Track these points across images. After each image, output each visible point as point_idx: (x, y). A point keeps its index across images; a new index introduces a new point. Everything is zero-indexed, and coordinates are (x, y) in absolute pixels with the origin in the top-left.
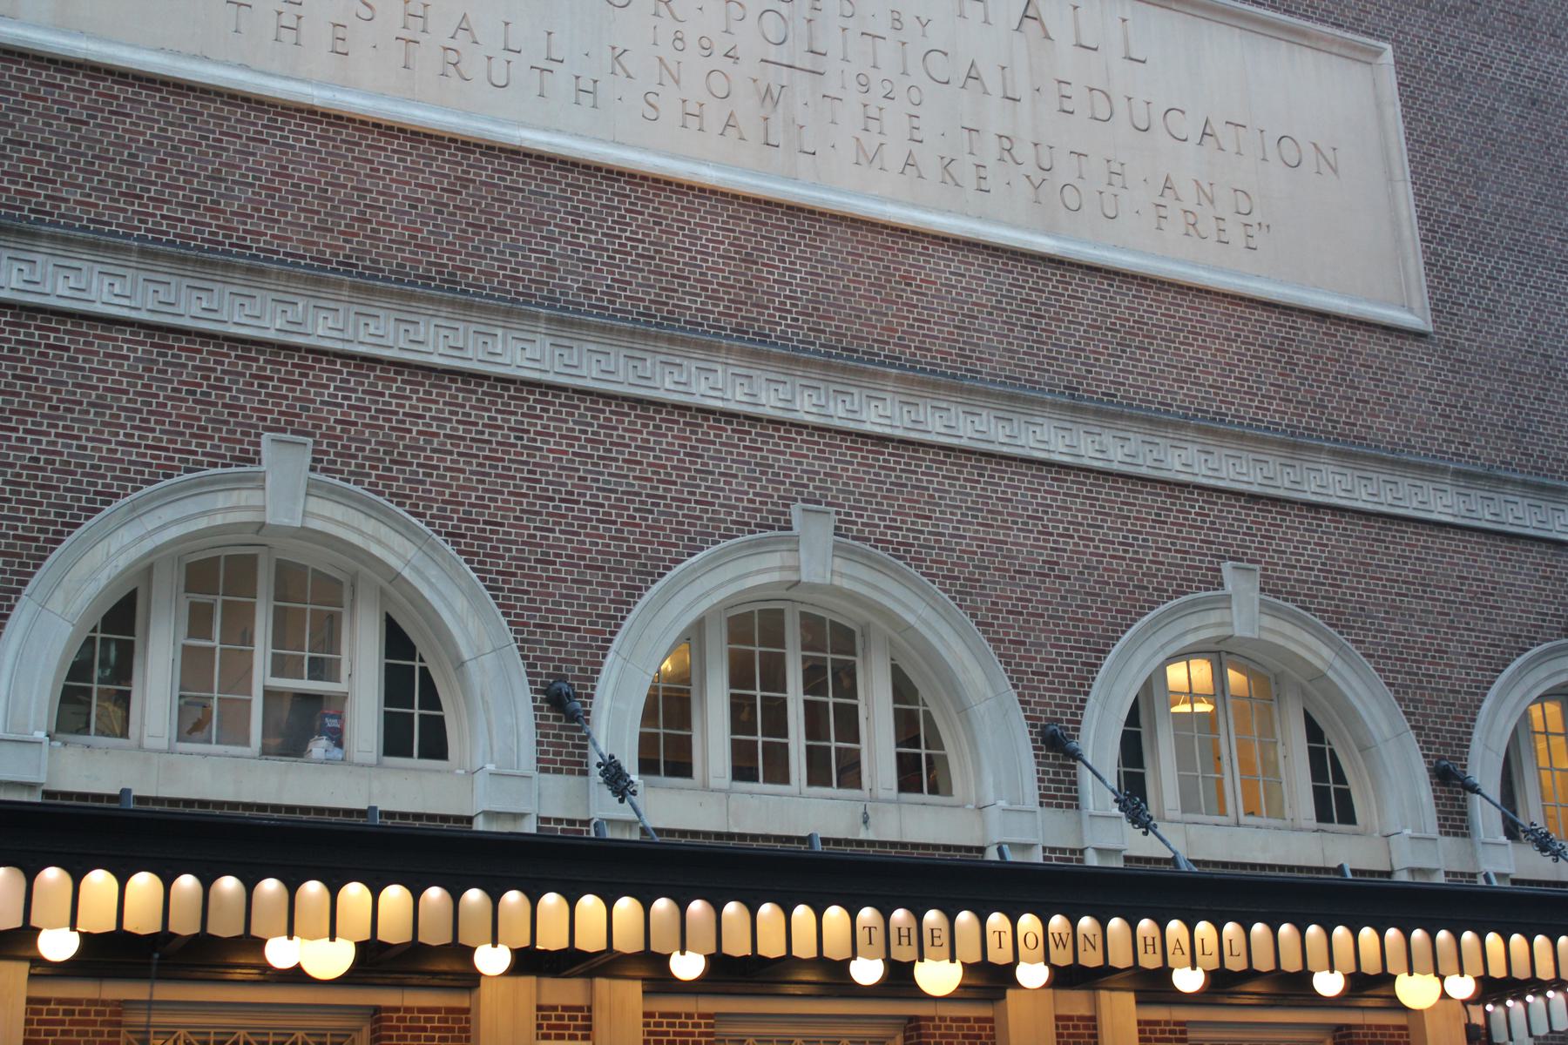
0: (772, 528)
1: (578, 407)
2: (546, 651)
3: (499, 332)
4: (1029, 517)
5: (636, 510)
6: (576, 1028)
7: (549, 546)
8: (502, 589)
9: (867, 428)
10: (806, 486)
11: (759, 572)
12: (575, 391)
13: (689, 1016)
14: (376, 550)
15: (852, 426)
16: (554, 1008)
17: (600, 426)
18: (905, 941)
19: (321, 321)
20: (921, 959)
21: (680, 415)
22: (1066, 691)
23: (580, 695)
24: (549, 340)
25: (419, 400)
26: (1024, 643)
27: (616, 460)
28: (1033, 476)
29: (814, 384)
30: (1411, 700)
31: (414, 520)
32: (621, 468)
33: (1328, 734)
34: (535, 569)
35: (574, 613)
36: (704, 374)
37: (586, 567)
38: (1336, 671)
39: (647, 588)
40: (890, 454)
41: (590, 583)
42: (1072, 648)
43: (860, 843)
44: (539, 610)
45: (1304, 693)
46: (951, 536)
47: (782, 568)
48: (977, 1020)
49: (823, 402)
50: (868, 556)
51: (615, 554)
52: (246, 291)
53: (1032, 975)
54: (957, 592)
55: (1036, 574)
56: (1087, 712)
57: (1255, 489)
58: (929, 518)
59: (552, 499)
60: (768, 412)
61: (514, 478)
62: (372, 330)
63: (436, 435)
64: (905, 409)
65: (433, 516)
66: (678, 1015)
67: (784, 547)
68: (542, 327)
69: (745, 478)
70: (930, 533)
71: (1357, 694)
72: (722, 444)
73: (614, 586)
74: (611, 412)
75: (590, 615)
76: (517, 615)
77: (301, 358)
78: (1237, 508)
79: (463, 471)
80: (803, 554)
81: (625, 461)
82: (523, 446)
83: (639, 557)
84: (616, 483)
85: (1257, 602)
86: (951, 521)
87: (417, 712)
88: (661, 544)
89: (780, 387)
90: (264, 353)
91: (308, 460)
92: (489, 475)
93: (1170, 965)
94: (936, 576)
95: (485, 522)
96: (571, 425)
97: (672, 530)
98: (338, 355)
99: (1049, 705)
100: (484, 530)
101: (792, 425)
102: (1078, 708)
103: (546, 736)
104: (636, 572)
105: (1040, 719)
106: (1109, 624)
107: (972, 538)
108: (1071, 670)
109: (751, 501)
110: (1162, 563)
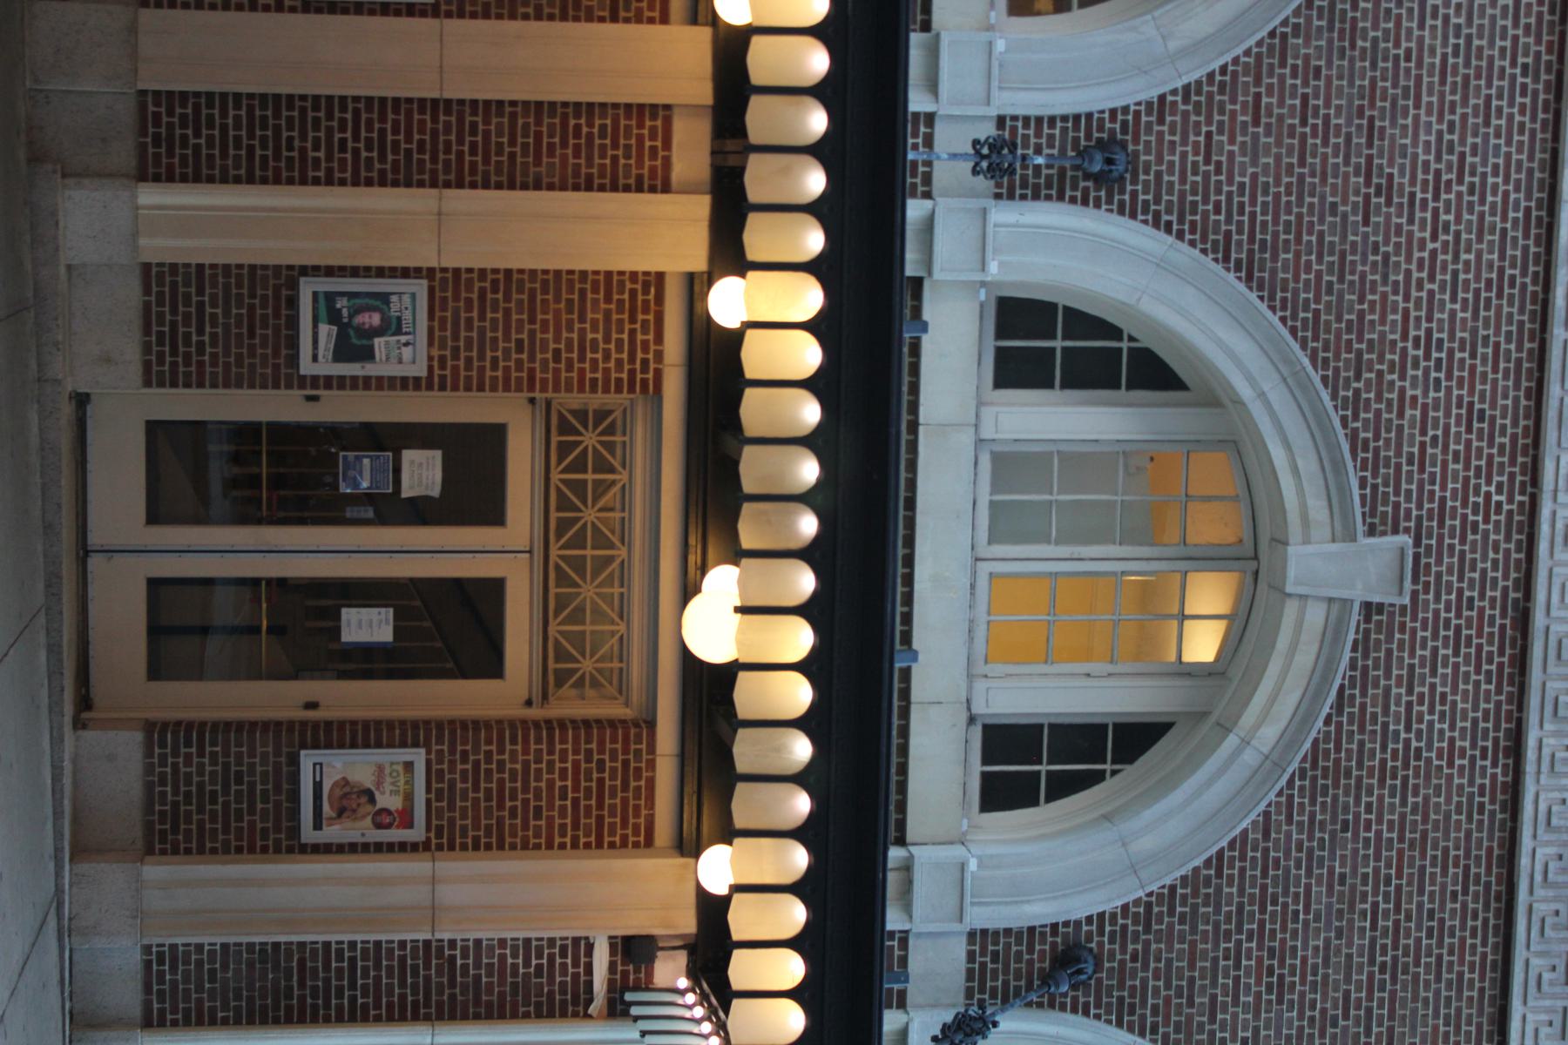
4: (1462, 156)
22: (1182, 194)
26: (1256, 123)
28: (1530, 171)
30: (1195, 907)
33: (1129, 771)
38: (1237, 752)
42: (1253, 215)
45: (1200, 716)
55: (1370, 158)
56: (1149, 230)
57: (1539, 620)
71: (1197, 794)
78: (1506, 582)
85: (1345, 594)
99: (1160, 160)
102: (1157, 215)
105: (1136, 141)
106: (1296, 292)
107: (1421, 39)
108: (1217, 211)
110: (1401, 415)
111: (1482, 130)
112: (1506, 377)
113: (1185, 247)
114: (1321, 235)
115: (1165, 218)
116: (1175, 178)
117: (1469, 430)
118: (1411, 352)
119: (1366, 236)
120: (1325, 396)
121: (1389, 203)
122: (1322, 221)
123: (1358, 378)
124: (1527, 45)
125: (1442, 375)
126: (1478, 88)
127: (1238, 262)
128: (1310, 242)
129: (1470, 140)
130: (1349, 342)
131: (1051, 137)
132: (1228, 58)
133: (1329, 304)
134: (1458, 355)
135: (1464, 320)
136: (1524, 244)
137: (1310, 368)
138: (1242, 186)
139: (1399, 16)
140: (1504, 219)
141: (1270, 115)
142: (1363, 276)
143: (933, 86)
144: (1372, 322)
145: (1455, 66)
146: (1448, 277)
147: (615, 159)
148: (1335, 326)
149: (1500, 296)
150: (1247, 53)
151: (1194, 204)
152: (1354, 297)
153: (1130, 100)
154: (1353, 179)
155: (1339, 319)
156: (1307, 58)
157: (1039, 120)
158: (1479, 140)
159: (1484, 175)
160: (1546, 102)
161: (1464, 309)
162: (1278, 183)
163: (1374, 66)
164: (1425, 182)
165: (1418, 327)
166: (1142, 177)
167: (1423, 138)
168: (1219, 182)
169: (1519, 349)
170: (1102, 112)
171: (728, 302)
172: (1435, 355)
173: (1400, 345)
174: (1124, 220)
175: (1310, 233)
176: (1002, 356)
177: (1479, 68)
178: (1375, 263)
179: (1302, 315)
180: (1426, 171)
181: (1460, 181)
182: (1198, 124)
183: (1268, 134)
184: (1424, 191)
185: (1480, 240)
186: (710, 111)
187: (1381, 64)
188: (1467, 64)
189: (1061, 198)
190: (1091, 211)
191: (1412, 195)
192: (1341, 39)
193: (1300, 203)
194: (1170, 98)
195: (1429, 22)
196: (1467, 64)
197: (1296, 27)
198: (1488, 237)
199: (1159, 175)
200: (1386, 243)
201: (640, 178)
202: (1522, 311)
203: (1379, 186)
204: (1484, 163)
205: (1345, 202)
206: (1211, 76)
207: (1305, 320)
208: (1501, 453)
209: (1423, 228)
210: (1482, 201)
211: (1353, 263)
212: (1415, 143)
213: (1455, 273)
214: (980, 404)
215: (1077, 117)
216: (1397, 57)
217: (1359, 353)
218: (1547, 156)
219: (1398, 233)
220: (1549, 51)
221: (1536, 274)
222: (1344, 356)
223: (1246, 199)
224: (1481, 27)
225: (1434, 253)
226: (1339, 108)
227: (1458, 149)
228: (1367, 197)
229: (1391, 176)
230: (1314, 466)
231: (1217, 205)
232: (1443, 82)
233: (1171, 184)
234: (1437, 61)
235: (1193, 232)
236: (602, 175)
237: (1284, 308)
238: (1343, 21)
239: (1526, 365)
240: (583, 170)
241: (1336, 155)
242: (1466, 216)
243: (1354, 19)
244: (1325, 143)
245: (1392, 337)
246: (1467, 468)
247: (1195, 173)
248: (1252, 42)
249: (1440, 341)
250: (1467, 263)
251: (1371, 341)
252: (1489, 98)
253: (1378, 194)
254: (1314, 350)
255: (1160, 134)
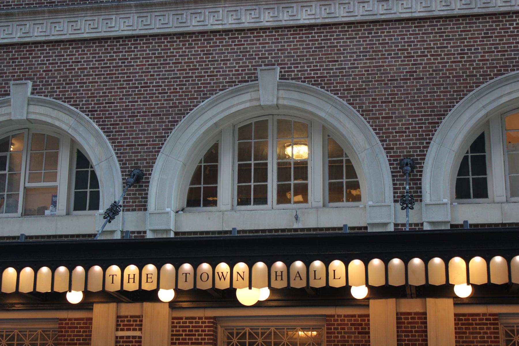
0: (247, 81)
1: (151, 43)
2: (131, 156)
3: (114, 17)
5: (177, 85)
6: (136, 325)
7: (135, 109)
8: (112, 132)
9: (301, 22)
10: (267, 58)
11: (238, 104)
12: (151, 36)
13: (200, 318)
14: (57, 123)
15: (292, 23)
16: (127, 317)
17: (162, 50)
18: (279, 278)
19: (36, 29)
20: (70, 291)
21: (214, 36)
22: (417, 139)
23: (146, 175)
24: (136, 16)
25: (79, 55)
26: (392, 117)
27: (169, 64)
28: (403, 28)
29: (272, 6)
31: (72, 108)
32: (172, 67)
34: (128, 120)
35: (145, 138)
36: (212, 14)
37: (152, 115)
39: (180, 121)
40: (315, 33)
41: (153, 123)
42: (422, 116)
43: (296, 230)
44: (129, 138)
46: (349, 68)
47: (251, 100)
48: (360, 316)
49: (276, 15)
50: (298, 86)
51: (166, 107)
52: (6, 24)
53: (166, 295)
54: (351, 97)
55: (401, 80)
56: (429, 149)
58: (337, 61)
59: (137, 87)
60: (246, 25)
61: (120, 81)
62: (57, 29)
63: (86, 68)
64: (323, 8)
65: (83, 105)
66: (194, 318)
67: (252, 90)
68: (134, 10)
69: (234, 60)
70: (336, 69)
72: (223, 46)
73: (165, 122)
74: (168, 42)
75: (152, 137)
76: (118, 142)
77: (30, 47)
79: (97, 82)
80: (261, 92)
81: (173, 63)
82: (125, 66)
83: (178, 107)
84: (168, 75)
86: (350, 60)
87: (88, 190)
88: (189, 99)
89: (253, 12)
90: (14, 48)
91: (30, 90)
92: (109, 82)
93: (350, 284)
94: (340, 90)
95: (106, 103)
96: (148, 52)
97: (195, 91)
98: (45, 42)
99: (406, 148)
100: (105, 107)
101: (261, 29)
102: (424, 147)
103: (129, 194)
104: (176, 114)
105: (400, 156)
106: (447, 99)
107: (361, 67)
108: (422, 127)
109: (236, 71)
110: (488, 60)
111: (390, 45)
112: (472, 27)
113: (434, 137)
114: (427, 93)
115: (425, 144)
116: (411, 142)
117: (492, 37)
118: (466, 59)
119: (427, 78)
120: (482, 86)
121: (416, 72)
122: (423, 93)
123: (476, 76)
124: (362, 34)
125: (473, 48)
126: (376, 47)
127: (438, 119)
128: (430, 96)
129: (393, 48)
130: (463, 80)
131: (400, 184)
132: (371, 128)
133: (451, 88)
134: (466, 44)
135: (454, 43)
136: (427, 27)
137: (473, 92)
138: (413, 120)
139: (355, 75)
140: (419, 34)
141: (389, 113)
142: (440, 78)
143: (385, 224)
144: (456, 73)
145: (369, 56)
146: (439, 50)
147: (416, 332)
148: (458, 85)
149: (445, 32)
150: (369, 122)
151: (420, 135)
152: (448, 80)
153: (386, 159)
154: (408, 84)
155: (456, 84)
156: (369, 103)
157: (394, 189)
158: (393, 45)
159: (404, 42)
160: (380, 26)
161: (450, 43)
162: (411, 108)
163: (371, 81)
164: (408, 61)
165: (457, 58)
166: (412, 153)
167: (393, 63)
168: (412, 128)
169: (462, 24)
170: (391, 168)
171: (463, 291)
172: (466, 51)
173: (463, 63)
174: (427, 158)
175: (427, 96)
176: (476, 196)
177: (370, 48)
178: (436, 74)
179: (455, 96)
180: (404, 61)
181: (407, 50)
182: (393, 136)
183: (395, 113)
184: (411, 61)
185: (426, 41)
186: (398, 299)
187: (370, 79)
188: (369, 52)
189: (420, 180)
190: (424, 169)
191: (413, 64)
192: (363, 93)
193: (417, 101)
194: (385, 146)
195: (356, 65)
196: (369, 52)
197: (359, 107)
198: (425, 39)
199: (410, 148)
200: (429, 71)
201: (422, 323)
202: (449, 25)
203: (410, 76)
204: (401, 43)
205: (416, 86)
206: (377, 134)
207: (457, 95)
208: (499, 25)
209: (423, 60)
210: (413, 42)
211: (436, 81)
212: (395, 65)
213: (438, 48)
214: (494, 202)
215: (393, 176)
216: (368, 74)
217: (467, 76)
218: (397, 23)
219: (426, 67)
220: (363, 26)
221: (436, 22)
222: (468, 81)
223: (417, 118)
224: (356, 49)
225: (431, 55)
226: (385, 91)
227: (396, 52)
228: (414, 79)
229: (407, 72)
230: (508, 87)
231: (419, 128)
232: (375, 59)
233: (413, 143)
234: (368, 61)
235: (429, 135)
236: (422, 336)
237: (453, 102)
238: (357, 93)
239: (468, 21)
240: (420, 342)
241: (401, 90)
242: (419, 46)
243: (356, 89)
244: (397, 94)
245: (461, 66)
246: (505, 36)
247: (409, 136)
248: (365, 121)
249: (461, 50)
250: (434, 44)
251: (463, 73)
252: (379, 44)
253: (413, 75)
254: (467, 91)
255: (397, 148)
